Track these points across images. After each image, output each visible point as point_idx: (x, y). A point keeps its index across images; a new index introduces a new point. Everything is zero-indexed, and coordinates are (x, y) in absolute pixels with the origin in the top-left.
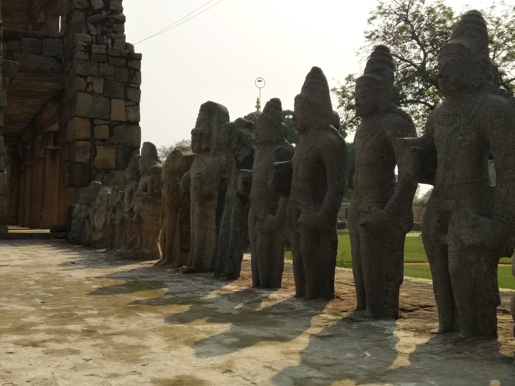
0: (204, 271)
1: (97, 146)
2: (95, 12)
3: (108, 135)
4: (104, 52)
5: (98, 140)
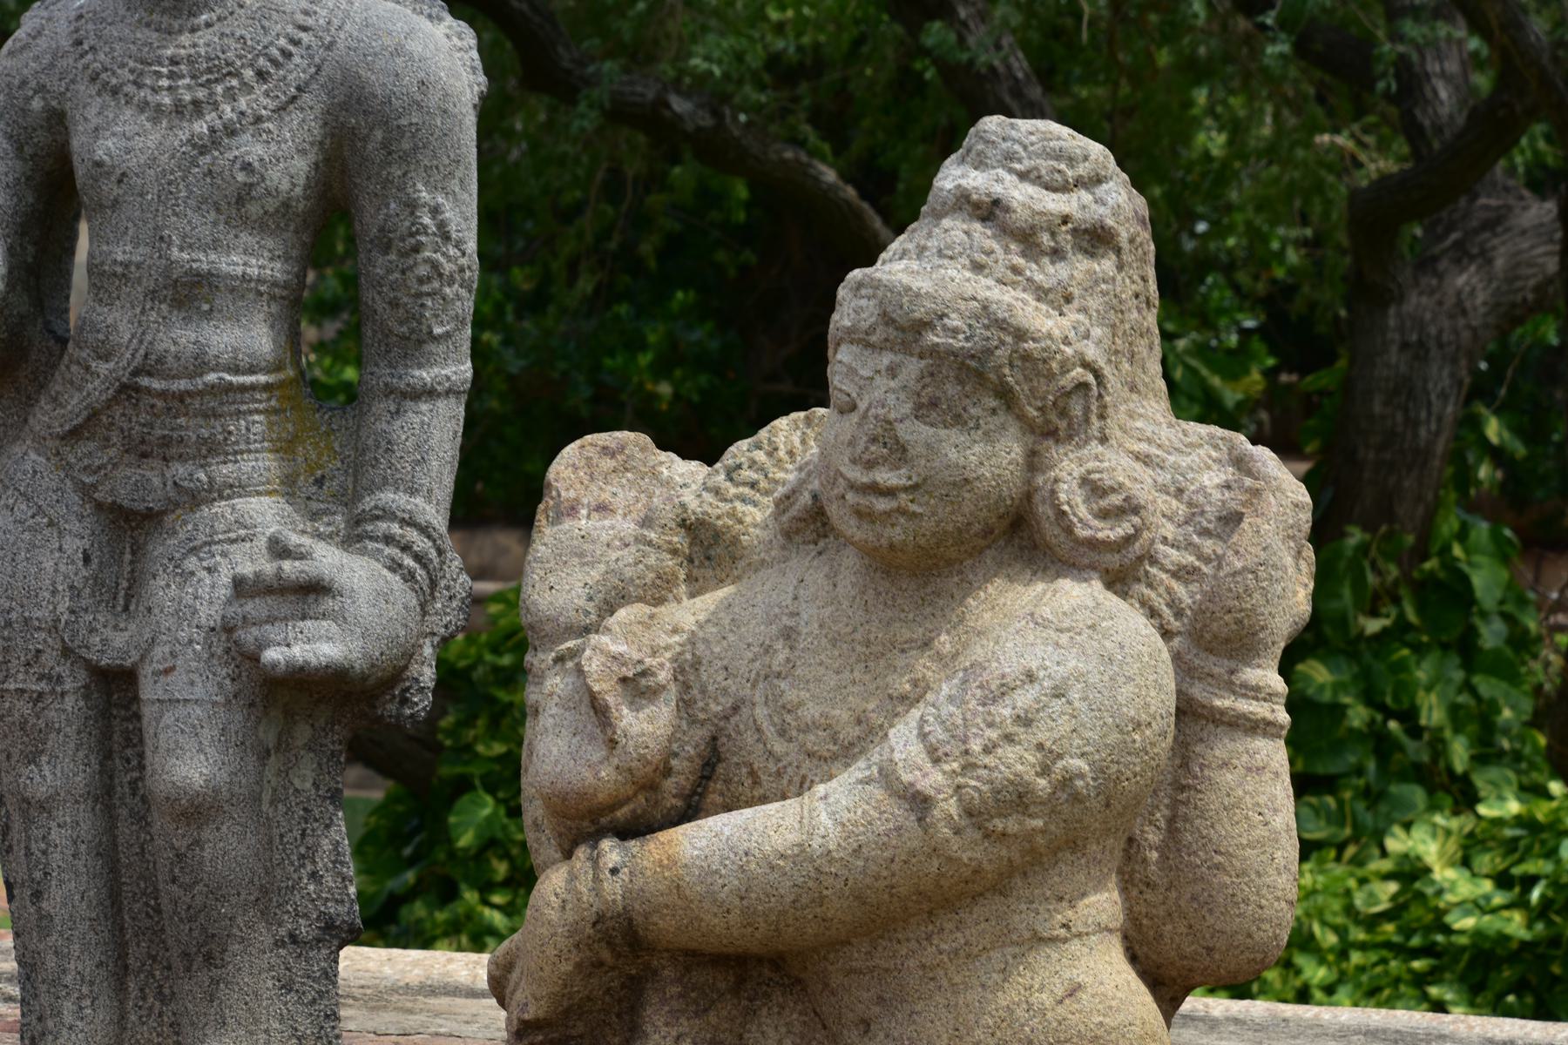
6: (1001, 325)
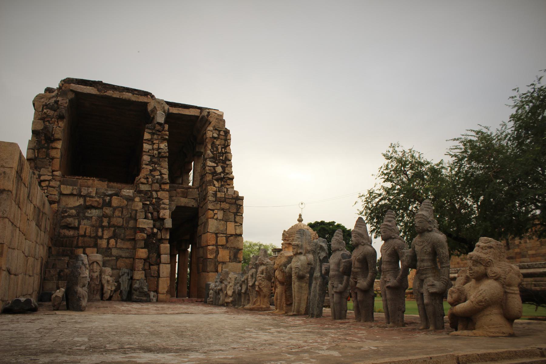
2: (217, 174)
4: (224, 196)
6: (478, 257)
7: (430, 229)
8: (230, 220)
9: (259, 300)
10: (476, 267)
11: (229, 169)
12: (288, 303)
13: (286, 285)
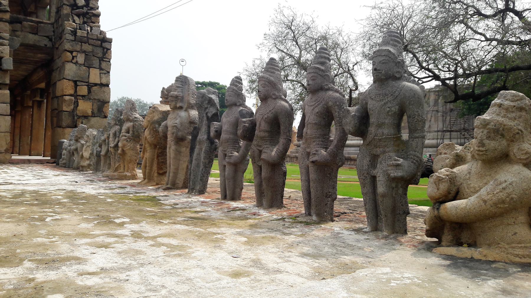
0: (178, 188)
1: (78, 100)
2: (78, 8)
3: (87, 92)
4: (86, 35)
5: (79, 96)
7: (398, 76)
8: (94, 66)
9: (122, 166)
10: (493, 142)
11: (94, 3)
12: (161, 172)
13: (159, 148)
